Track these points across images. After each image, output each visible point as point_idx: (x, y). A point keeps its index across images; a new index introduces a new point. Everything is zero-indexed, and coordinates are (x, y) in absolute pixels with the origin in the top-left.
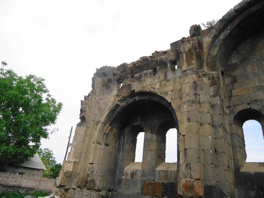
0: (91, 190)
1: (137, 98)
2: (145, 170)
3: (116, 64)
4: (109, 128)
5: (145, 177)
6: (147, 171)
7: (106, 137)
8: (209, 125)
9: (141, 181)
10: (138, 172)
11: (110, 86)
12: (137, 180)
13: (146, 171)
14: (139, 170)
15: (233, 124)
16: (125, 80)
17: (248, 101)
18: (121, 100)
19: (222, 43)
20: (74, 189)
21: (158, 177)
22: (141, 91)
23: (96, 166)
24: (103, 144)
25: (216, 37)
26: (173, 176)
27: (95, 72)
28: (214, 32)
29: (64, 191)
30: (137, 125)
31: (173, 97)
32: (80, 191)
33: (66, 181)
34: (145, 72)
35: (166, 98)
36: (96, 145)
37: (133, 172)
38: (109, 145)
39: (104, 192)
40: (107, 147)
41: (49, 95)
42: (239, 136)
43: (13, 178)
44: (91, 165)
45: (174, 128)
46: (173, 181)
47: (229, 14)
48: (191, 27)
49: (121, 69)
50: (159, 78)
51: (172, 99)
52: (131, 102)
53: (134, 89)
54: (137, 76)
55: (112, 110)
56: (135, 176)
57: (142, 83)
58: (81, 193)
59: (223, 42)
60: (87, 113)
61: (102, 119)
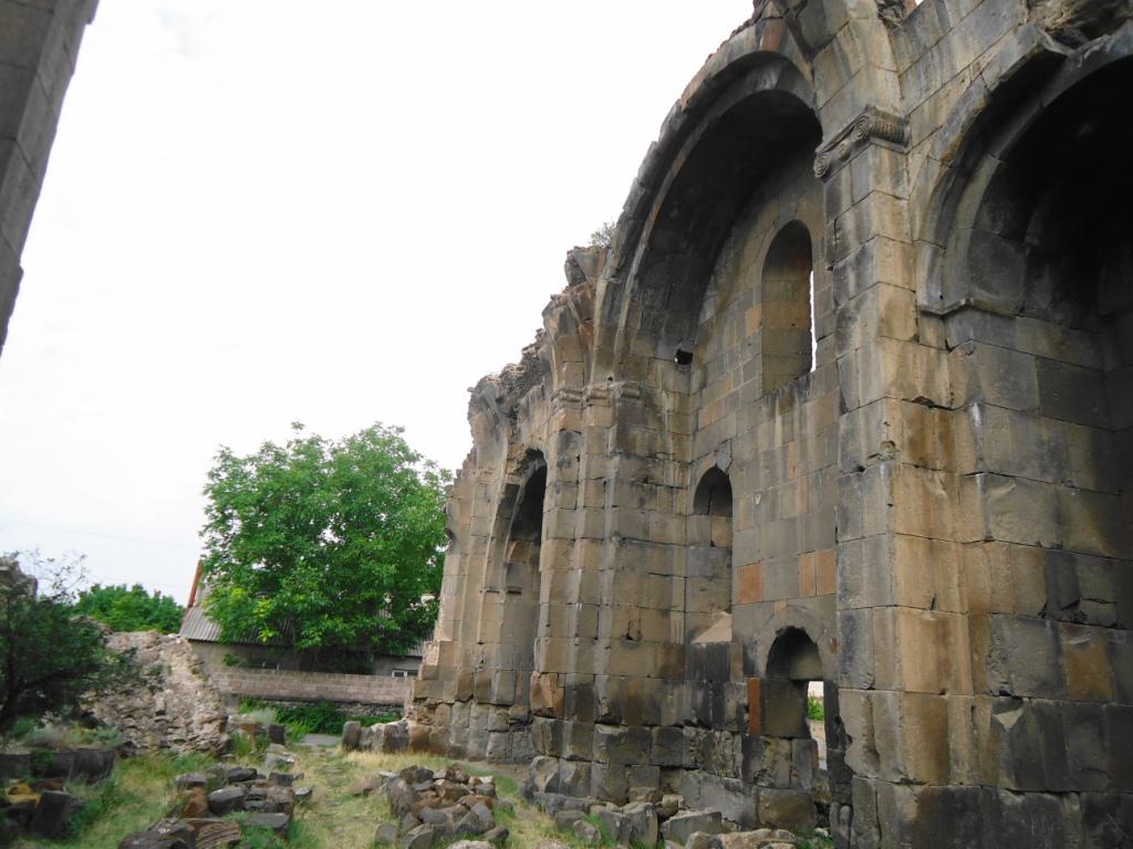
0: (486, 706)
3: (496, 370)
4: (512, 548)
7: (509, 572)
8: (584, 541)
15: (694, 514)
17: (716, 444)
18: (518, 470)
19: (636, 287)
20: (451, 705)
23: (493, 649)
24: (503, 592)
25: (621, 270)
27: (469, 399)
28: (612, 261)
29: (425, 709)
32: (462, 707)
33: (424, 689)
36: (485, 598)
38: (523, 591)
39: (520, 708)
40: (516, 598)
41: (430, 464)
42: (713, 545)
43: (381, 686)
44: (481, 648)
47: (630, 202)
48: (576, 248)
55: (503, 501)
58: (466, 712)
59: (637, 282)
60: (456, 518)
61: (491, 528)
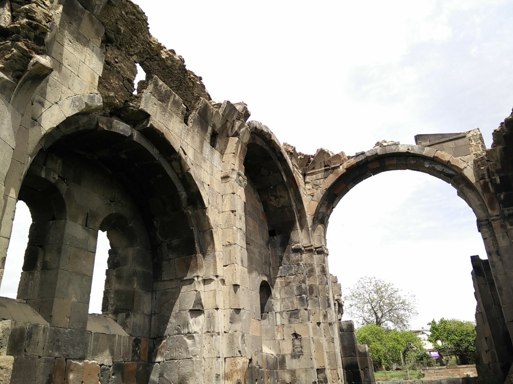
1: (136, 136)
2: (62, 329)
5: (58, 348)
6: (66, 331)
9: (47, 361)
10: (37, 334)
11: (80, 20)
12: (33, 359)
13: (65, 333)
14: (43, 326)
16: (121, 55)
21: (93, 350)
22: (163, 134)
26: (122, 348)
30: (46, 181)
31: (210, 201)
34: (177, 97)
35: (203, 194)
37: (22, 331)
45: (103, 231)
46: (122, 360)
49: (127, 13)
50: (193, 137)
51: (209, 203)
52: (122, 133)
53: (149, 112)
54: (161, 86)
56: (29, 345)
57: (166, 116)
